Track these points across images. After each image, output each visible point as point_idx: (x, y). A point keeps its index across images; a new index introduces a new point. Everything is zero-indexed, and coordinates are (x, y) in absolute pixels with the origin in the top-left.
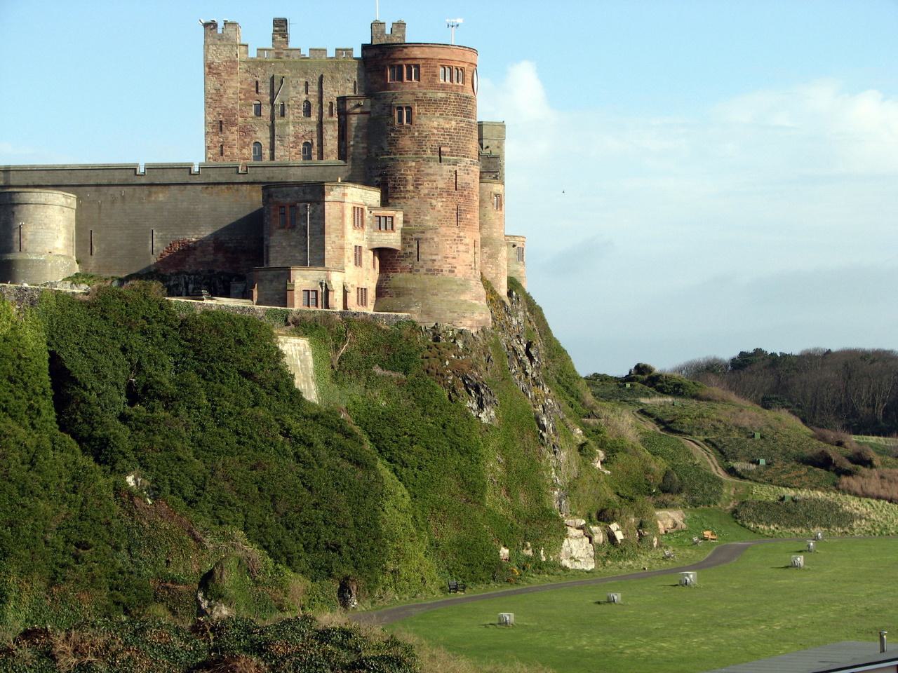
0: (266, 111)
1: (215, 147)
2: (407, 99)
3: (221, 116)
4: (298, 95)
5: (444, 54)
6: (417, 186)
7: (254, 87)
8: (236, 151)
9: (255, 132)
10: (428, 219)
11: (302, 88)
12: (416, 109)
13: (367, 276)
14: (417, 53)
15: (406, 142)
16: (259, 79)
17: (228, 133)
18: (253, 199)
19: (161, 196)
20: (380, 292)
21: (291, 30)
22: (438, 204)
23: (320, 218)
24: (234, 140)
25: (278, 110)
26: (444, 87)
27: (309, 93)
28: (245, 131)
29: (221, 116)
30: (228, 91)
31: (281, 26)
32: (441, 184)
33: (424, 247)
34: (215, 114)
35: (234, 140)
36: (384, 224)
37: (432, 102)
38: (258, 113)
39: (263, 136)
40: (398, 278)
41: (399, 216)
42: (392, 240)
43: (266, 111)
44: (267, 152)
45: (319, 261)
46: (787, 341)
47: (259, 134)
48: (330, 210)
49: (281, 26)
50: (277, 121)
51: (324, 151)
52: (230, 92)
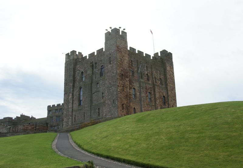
1: (121, 86)
3: (123, 72)
4: (144, 71)
7: (130, 62)
8: (128, 90)
9: (133, 83)
11: (146, 68)
16: (132, 59)
17: (125, 80)
24: (127, 85)
27: (148, 71)
29: (123, 72)
30: (125, 61)
34: (120, 70)
35: (127, 85)
47: (135, 84)
51: (156, 97)
52: (126, 61)
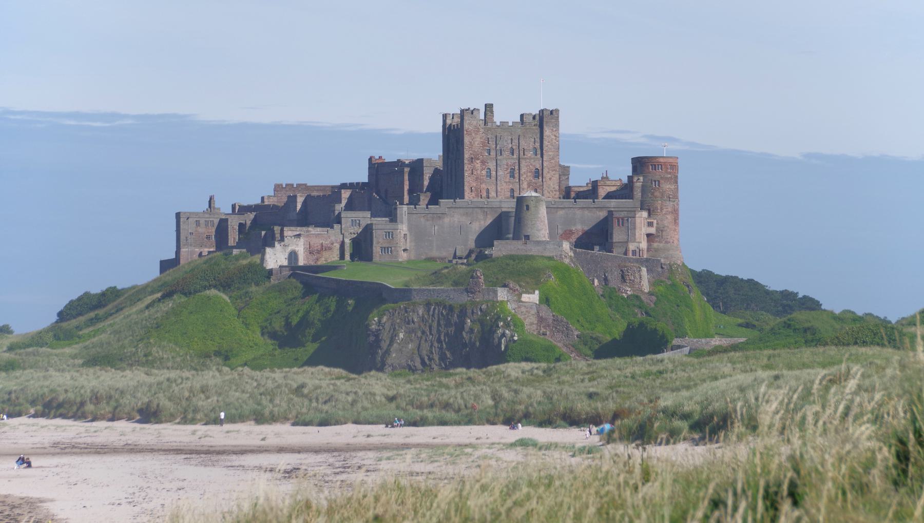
0: (493, 153)
2: (657, 178)
5: (671, 160)
6: (662, 209)
10: (666, 223)
11: (509, 141)
12: (662, 181)
13: (644, 245)
14: (662, 160)
15: (657, 194)
18: (603, 214)
19: (561, 212)
20: (649, 250)
21: (495, 109)
22: (669, 217)
23: (635, 223)
25: (499, 152)
26: (670, 173)
28: (483, 162)
31: (489, 108)
32: (670, 210)
33: (664, 233)
36: (650, 224)
37: (667, 178)
38: (489, 152)
39: (492, 165)
40: (655, 245)
41: (655, 222)
42: (652, 230)
43: (493, 153)
44: (494, 173)
45: (634, 241)
46: (721, 269)
48: (638, 220)
49: (489, 108)
50: (499, 158)
